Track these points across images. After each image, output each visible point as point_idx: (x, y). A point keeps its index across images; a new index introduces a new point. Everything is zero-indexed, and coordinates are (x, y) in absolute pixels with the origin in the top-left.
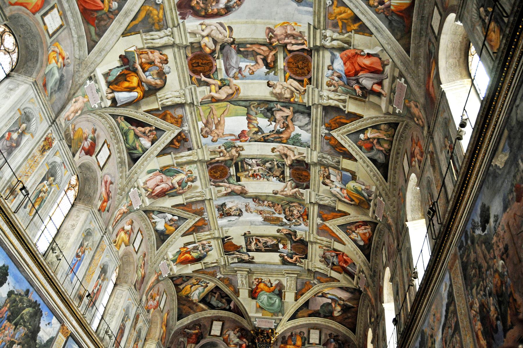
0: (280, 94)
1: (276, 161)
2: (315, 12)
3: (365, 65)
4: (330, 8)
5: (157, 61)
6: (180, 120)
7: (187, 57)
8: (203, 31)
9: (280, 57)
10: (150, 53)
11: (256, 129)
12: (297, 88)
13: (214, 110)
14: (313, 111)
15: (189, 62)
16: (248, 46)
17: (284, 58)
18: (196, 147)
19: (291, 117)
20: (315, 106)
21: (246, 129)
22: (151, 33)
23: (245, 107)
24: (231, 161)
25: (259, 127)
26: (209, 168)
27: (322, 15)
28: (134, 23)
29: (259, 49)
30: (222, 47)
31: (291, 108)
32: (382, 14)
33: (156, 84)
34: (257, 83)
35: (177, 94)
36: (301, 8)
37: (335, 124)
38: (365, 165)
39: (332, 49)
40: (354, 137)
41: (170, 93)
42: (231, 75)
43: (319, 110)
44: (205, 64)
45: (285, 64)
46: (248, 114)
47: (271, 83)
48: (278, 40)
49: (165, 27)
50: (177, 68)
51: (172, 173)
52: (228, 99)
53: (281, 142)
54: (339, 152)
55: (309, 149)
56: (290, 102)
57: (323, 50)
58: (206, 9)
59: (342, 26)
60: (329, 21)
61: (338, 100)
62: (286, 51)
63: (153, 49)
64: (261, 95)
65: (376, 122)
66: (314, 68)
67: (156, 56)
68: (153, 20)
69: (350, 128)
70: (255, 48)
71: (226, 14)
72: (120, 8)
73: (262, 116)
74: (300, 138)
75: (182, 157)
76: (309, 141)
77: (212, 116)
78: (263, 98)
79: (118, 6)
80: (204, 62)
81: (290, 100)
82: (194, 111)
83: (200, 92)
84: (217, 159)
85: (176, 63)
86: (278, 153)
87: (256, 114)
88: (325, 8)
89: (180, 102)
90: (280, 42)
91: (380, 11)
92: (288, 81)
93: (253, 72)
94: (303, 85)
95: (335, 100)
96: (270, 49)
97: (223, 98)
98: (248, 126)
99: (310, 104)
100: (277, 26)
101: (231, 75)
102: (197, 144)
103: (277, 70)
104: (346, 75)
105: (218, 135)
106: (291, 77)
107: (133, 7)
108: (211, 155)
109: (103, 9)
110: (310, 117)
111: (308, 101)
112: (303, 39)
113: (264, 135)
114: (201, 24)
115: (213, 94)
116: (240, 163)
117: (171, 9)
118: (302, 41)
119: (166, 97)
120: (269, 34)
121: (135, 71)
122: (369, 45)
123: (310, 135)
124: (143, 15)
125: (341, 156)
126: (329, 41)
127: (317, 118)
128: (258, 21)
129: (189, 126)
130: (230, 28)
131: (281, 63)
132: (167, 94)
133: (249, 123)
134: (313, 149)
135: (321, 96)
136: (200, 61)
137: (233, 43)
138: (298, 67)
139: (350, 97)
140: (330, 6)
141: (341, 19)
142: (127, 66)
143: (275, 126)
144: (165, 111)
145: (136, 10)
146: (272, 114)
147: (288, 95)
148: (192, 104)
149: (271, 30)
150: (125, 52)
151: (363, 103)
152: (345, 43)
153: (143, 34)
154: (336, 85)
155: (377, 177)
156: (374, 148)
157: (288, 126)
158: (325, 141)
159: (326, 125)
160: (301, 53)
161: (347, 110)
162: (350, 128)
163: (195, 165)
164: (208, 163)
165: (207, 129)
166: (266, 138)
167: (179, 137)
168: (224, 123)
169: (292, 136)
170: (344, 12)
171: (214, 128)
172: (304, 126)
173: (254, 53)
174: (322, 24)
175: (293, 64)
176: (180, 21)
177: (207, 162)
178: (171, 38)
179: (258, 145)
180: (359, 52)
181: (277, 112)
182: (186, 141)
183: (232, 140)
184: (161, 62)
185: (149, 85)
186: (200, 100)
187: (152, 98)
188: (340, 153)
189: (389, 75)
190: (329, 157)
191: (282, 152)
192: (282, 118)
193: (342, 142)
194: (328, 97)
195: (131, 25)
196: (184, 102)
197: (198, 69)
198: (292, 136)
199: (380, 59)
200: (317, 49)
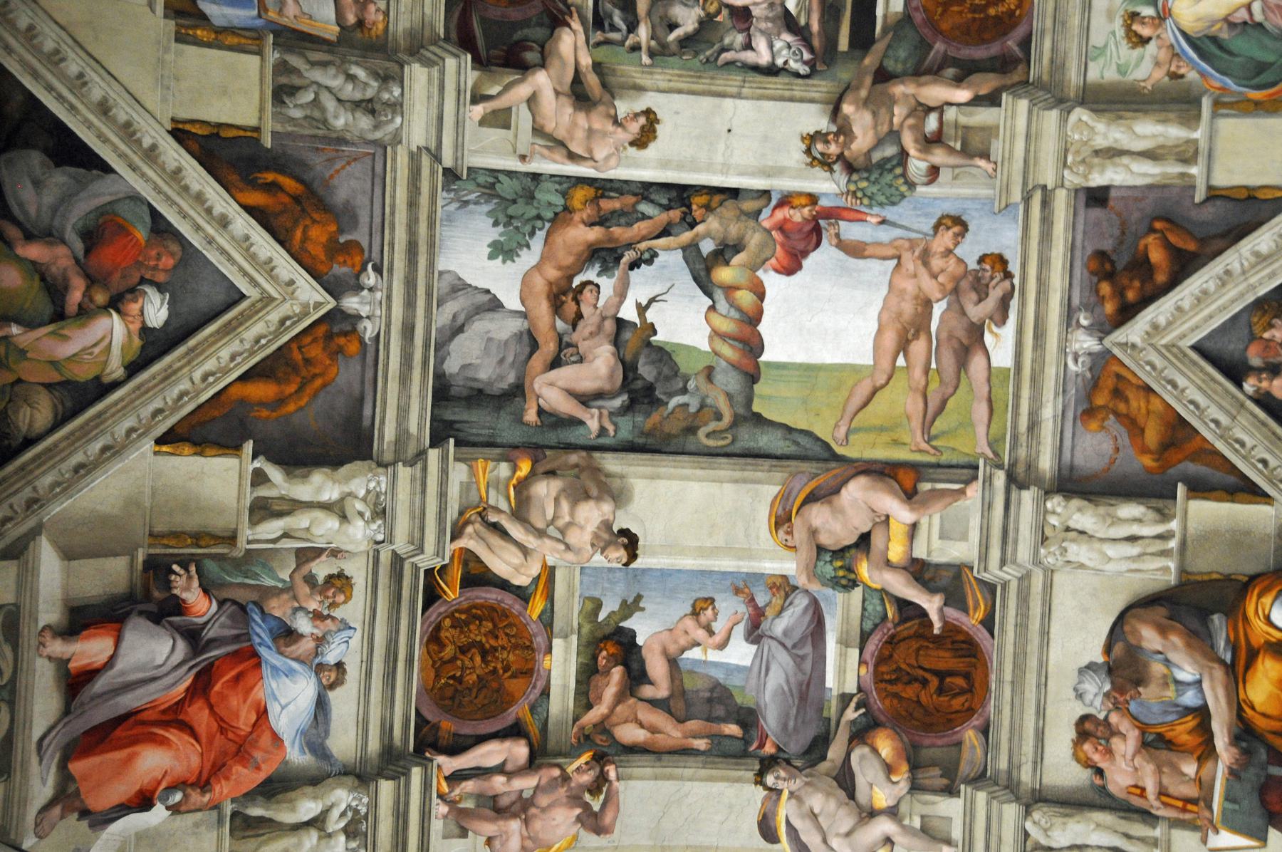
0: (579, 495)
1: (636, 48)
3: (163, 742)
5: (1126, 746)
6: (1100, 400)
7: (985, 731)
8: (888, 841)
9: (565, 675)
11: (724, 274)
12: (495, 540)
13: (916, 423)
14: (419, 422)
15: (984, 701)
16: (701, 744)
17: (546, 693)
18: (1061, 201)
19: (538, 361)
20: (411, 450)
21: (773, 282)
23: (758, 420)
24: (890, 65)
25: (705, 285)
26: (1020, 32)
29: (653, 730)
30: (817, 749)
31: (531, 416)
33: (1163, 631)
34: (683, 551)
35: (1079, 552)
37: (307, 361)
38: (123, 111)
40: (209, 295)
41: (1110, 567)
42: (801, 602)
43: (390, 433)
44: (912, 680)
45: (546, 664)
46: (752, 376)
47: (622, 554)
48: (565, 778)
50: (1042, 685)
51: (1246, 47)
52: (836, 469)
53: (602, 188)
54: (281, 170)
55: (448, 161)
56: (535, 450)
61: (296, 506)
62: (534, 730)
64: (675, 485)
65: (85, 434)
69: (225, 354)
70: (673, 733)
73: (680, 360)
74: (495, 234)
75: (1150, 155)
76: (449, 219)
77: (934, 385)
78: (665, 465)
80: (910, 692)
81: (535, 462)
82: (1015, 438)
83: (964, 537)
84: (963, 95)
85: (1041, 713)
86: (623, 107)
87: (709, 373)
89: (1076, 502)
90: (556, 772)
92: (535, 569)
93: (695, 613)
94: (468, 557)
95: (310, 505)
97: (862, 481)
98: (761, 295)
99: (433, 455)
100: (563, 843)
101: (801, 602)
102: (1047, 221)
103: (586, 629)
104: (255, 655)
105: (925, 258)
106: (523, 594)
108: (990, 131)
110: (440, 376)
111: (444, 472)
112: (452, 803)
113: (687, 236)
115: (902, 514)
116: (844, 43)
118: (457, 791)
119: (1134, 550)
121: (1245, 733)
123: (441, 265)
125: (267, 142)
126: (335, 813)
127: (404, 379)
129: (1063, 351)
130: (767, 830)
132: (1124, 566)
133: (754, 318)
134: (426, 161)
135: (380, 513)
136: (928, 696)
137: (767, 764)
138: (484, 653)
139: (232, 539)
143: (622, 295)
144: (1164, 468)
146: (629, 368)
147: (545, 490)
148: (1015, 481)
149: (594, 822)
150: (1263, 839)
151: (159, 528)
152: (262, 821)
154: (304, 590)
155: (36, 50)
156: (79, 246)
157: (557, 307)
158: (361, 236)
159: (353, 347)
160: (468, 729)
161: (246, 461)
162: (225, 354)
163: (1093, 75)
164: (1016, 77)
165: (976, 312)
166: (675, 214)
167: (1131, 295)
168: (880, 332)
169: (541, 235)
171: (938, 309)
172: (469, 318)
173: (678, 706)
177: (1024, 86)
179: (726, 169)
180: (196, 798)
181: (607, 387)
182: (1101, 255)
183: (858, 218)
184: (1113, 732)
185: (1200, 640)
186: (974, 491)
187: (1208, 563)
188: (278, 161)
189: (34, 759)
190: (341, 120)
191: (598, 121)
192: (583, 346)
193: (265, 245)
194: (344, 517)
196: (1055, 503)
198: (541, 235)
199: (85, 813)
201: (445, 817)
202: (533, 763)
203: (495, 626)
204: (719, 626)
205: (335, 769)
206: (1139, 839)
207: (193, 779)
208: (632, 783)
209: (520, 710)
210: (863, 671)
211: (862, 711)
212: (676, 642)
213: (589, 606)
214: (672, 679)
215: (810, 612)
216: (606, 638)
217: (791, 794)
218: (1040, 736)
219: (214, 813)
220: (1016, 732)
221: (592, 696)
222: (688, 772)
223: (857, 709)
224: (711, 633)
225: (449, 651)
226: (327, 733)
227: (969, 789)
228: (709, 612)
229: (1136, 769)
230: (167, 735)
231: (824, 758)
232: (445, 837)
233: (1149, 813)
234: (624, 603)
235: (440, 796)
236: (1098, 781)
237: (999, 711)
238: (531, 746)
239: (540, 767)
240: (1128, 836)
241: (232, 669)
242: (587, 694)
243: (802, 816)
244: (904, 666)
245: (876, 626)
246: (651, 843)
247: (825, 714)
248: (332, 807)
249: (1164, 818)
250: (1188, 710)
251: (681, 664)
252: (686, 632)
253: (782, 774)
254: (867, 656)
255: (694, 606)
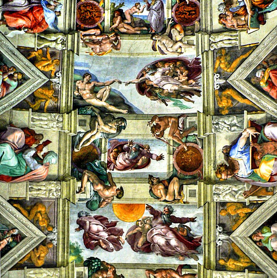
2: (72, 66)
3: (23, 19)
4: (59, 70)
7: (199, 21)
8: (180, 47)
10: (235, 25)
15: (199, 15)
16: (139, 32)
17: (104, 21)
22: (231, 46)
27: (65, 64)
28: (244, 57)
29: (128, 29)
32: (10, 67)
36: (85, 69)
39: (56, 32)
44: (183, 13)
48: (109, 38)
49: (216, 51)
50: (211, 10)
57: (65, 30)
58: (175, 67)
59: (47, 53)
60: (59, 58)
62: (101, 28)
63: (230, 31)
66: (74, 12)
67: (230, 22)
68: (226, 58)
70: (132, 30)
71: (156, 63)
72: (255, 71)
79: (256, 73)
80: (183, 16)
85: (211, 15)
88: (62, 69)
90: (107, 37)
91: (12, 69)
93: (136, 6)
96: (117, 29)
100: (109, 51)
103: (112, 9)
107: (242, 71)
109: (271, 71)
114: (181, 53)
117: (207, 68)
118: (85, 38)
120: (118, 44)
122: (20, 38)
124: (235, 64)
126: (59, 40)
128: (127, 56)
130: (154, 48)
131: (107, 16)
137: (153, 35)
138: (90, 13)
140: (58, 72)
141: (48, 60)
142: (259, 12)
145: (240, 69)
149: (116, 47)
152: (44, 38)
153: (238, 45)
170: (44, 67)
174: (66, 55)
175: (95, 15)
176: (200, 57)
178: (212, 40)
180: (30, 31)
195: (248, 54)
197: (190, 9)
200: (71, 31)
201: (82, 43)
202: (101, 34)
203: (92, 7)
204: (141, 8)
205: (59, 31)
206: (234, 36)
207: (29, 27)
208: (124, 40)
209: (98, 24)
210: (172, 14)
211: (173, 21)
212: (132, 12)
213: (112, 4)
214: (131, 19)
215: (161, 3)
216: (116, 11)
217: (159, 40)
218: (211, 20)
219: (34, 35)
220: (206, 20)
221: (114, 22)
222: (136, 38)
223: (172, 21)
224: (140, 10)
225: (83, 11)
226: (57, 24)
227: (197, 34)
228: (139, 6)
229: (232, 22)
230: (24, 18)
231: (165, 32)
232: (82, 47)
233: (236, 30)
234: (120, 4)
235: (81, 39)
236: (224, 26)
237: (202, 17)
238: (101, 30)
239: (102, 35)
240: (231, 36)
241: (37, 9)
242: (113, 22)
243: (161, 45)
244: (181, 11)
245: (175, 4)
246: (129, 52)
247: (165, 23)
248: (59, 38)
249: (239, 30)
250: (242, 7)
251: (133, 16)
252: (134, 10)
253: (156, 37)
254: (173, 10)
255: (135, 5)
